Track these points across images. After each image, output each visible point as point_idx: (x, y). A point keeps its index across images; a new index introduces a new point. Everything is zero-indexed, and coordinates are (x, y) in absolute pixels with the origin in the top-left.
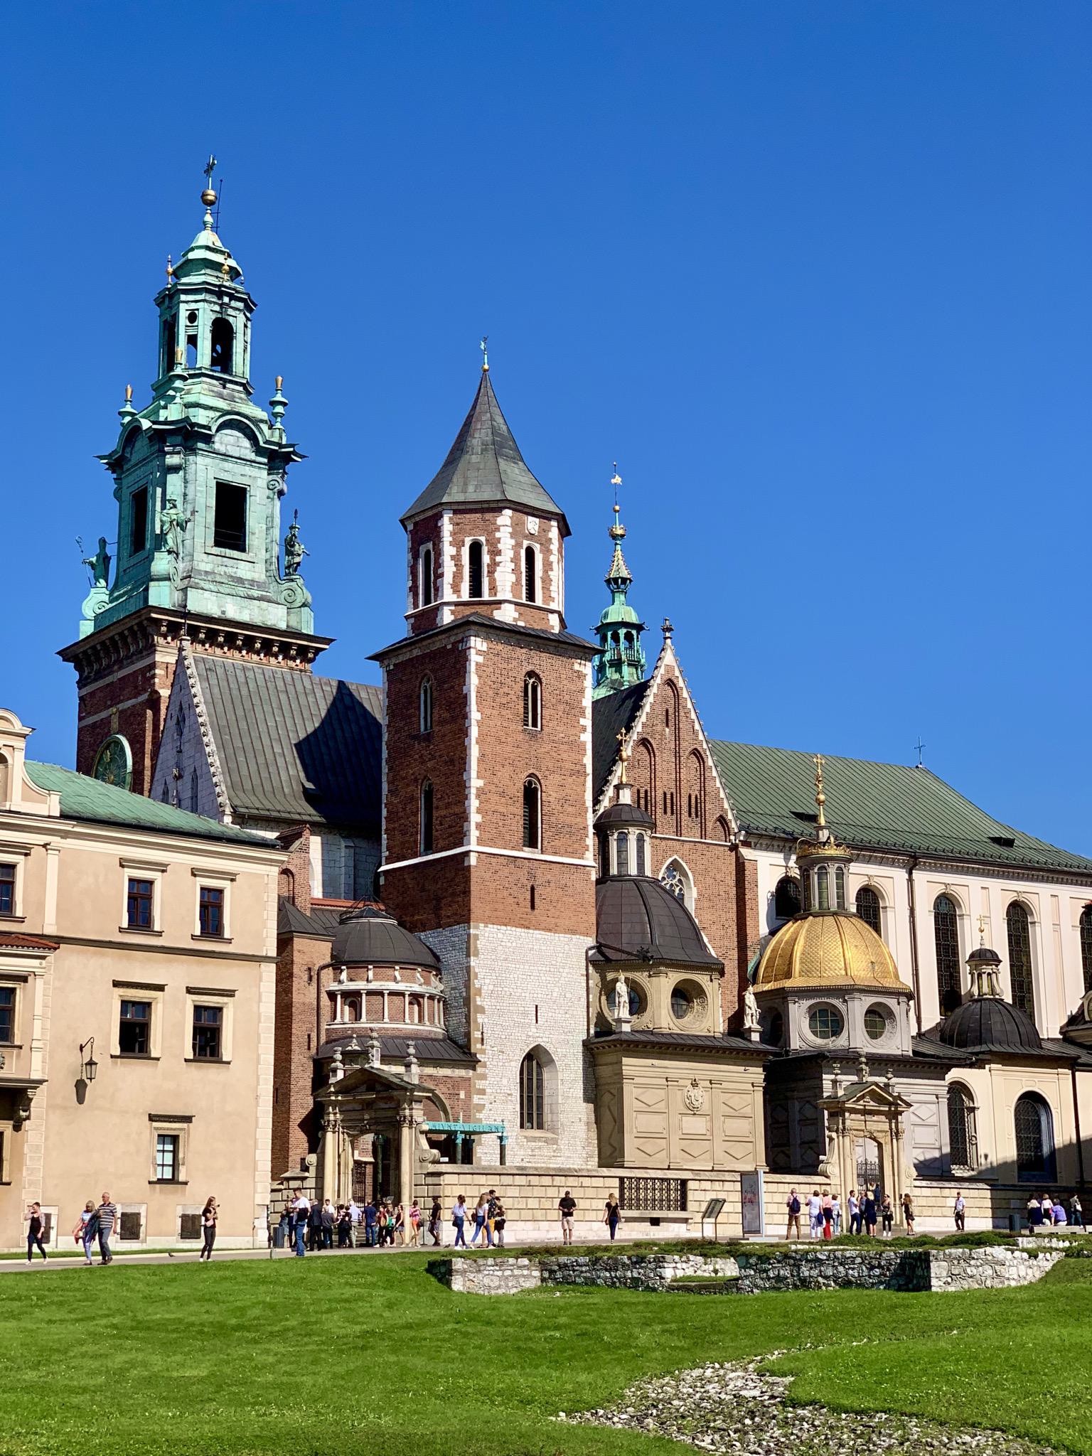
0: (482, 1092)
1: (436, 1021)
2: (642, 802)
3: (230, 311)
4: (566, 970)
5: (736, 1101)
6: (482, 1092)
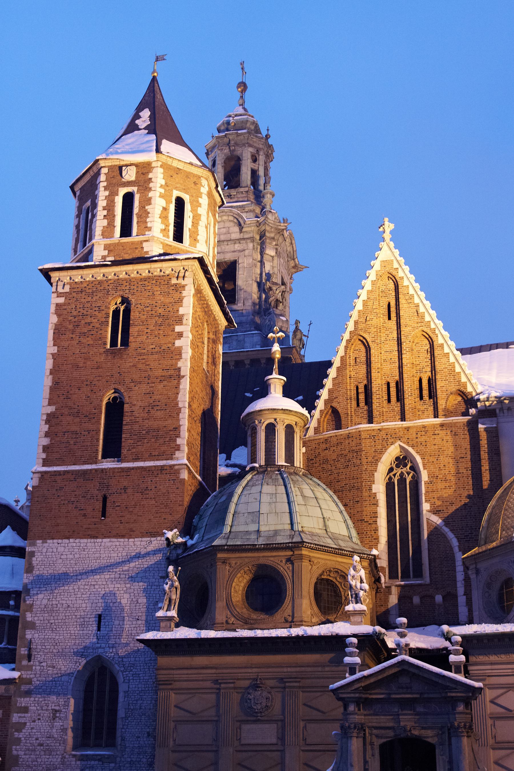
0: (25, 710)
2: (362, 397)
6: (25, 710)
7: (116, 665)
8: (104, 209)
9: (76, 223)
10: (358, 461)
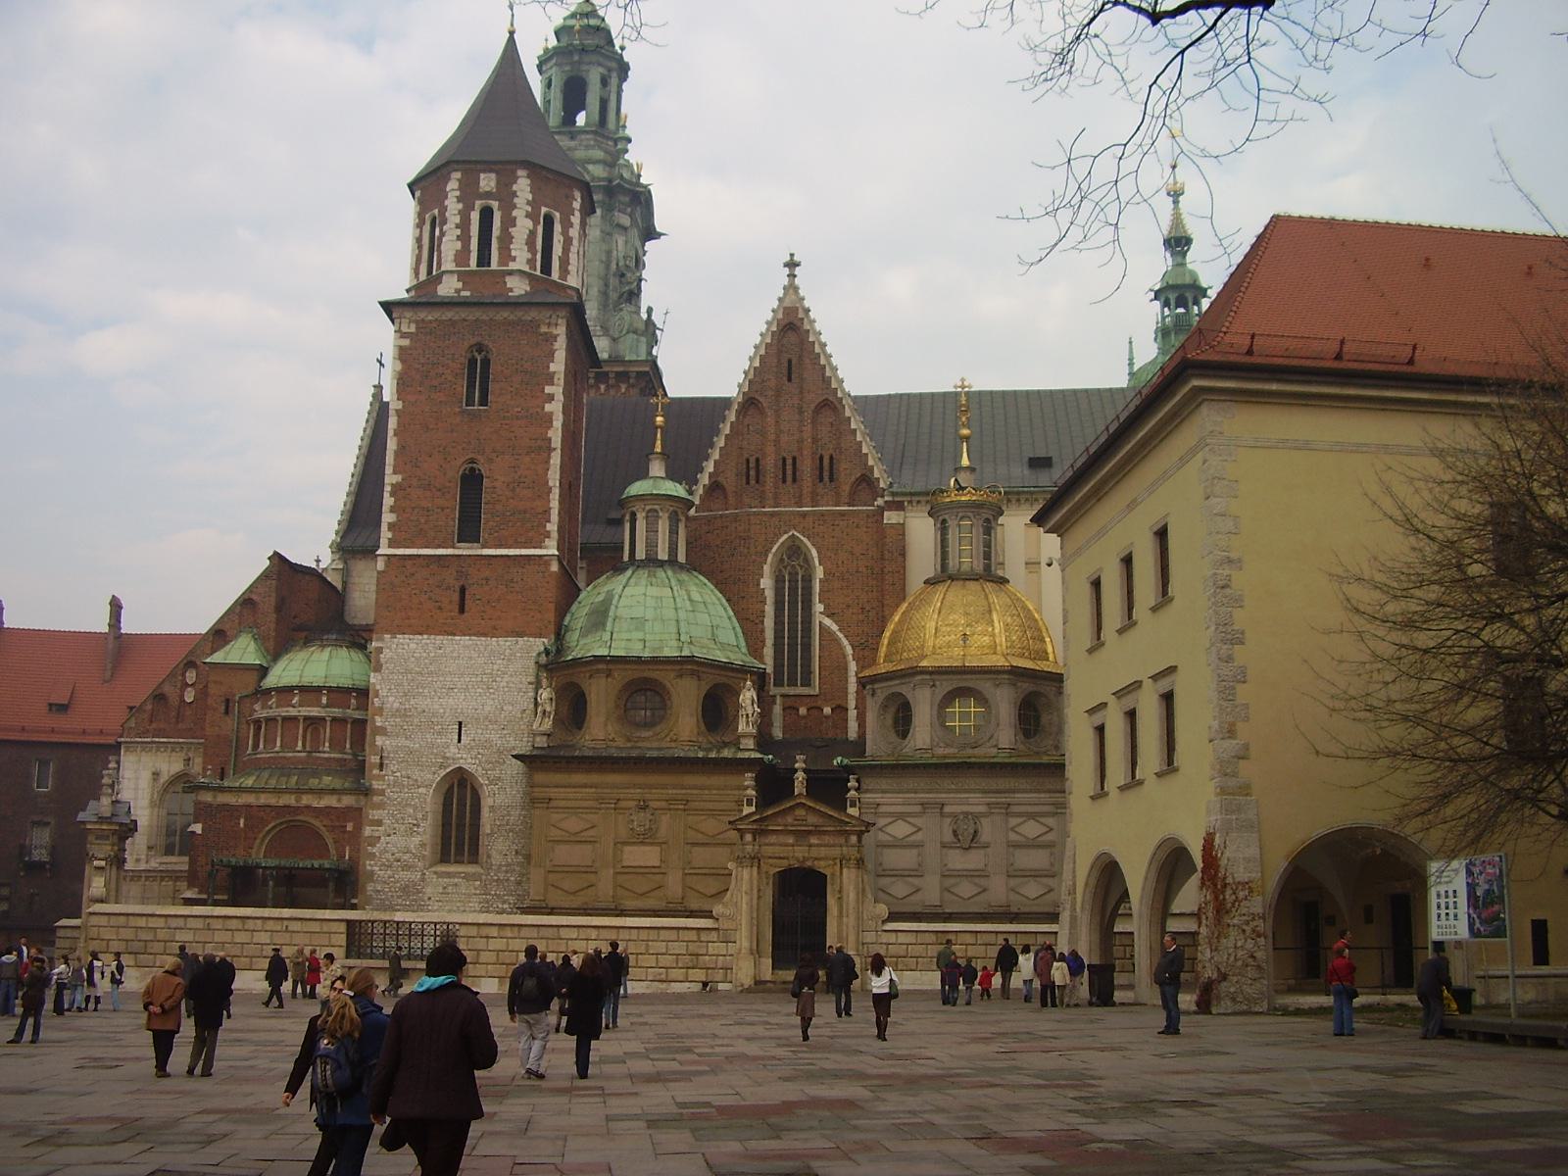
0: (379, 823)
1: (348, 746)
2: (752, 473)
3: (585, 67)
4: (505, 680)
5: (711, 826)
6: (379, 823)
7: (480, 779)
8: (457, 227)
9: (417, 235)
10: (746, 551)
